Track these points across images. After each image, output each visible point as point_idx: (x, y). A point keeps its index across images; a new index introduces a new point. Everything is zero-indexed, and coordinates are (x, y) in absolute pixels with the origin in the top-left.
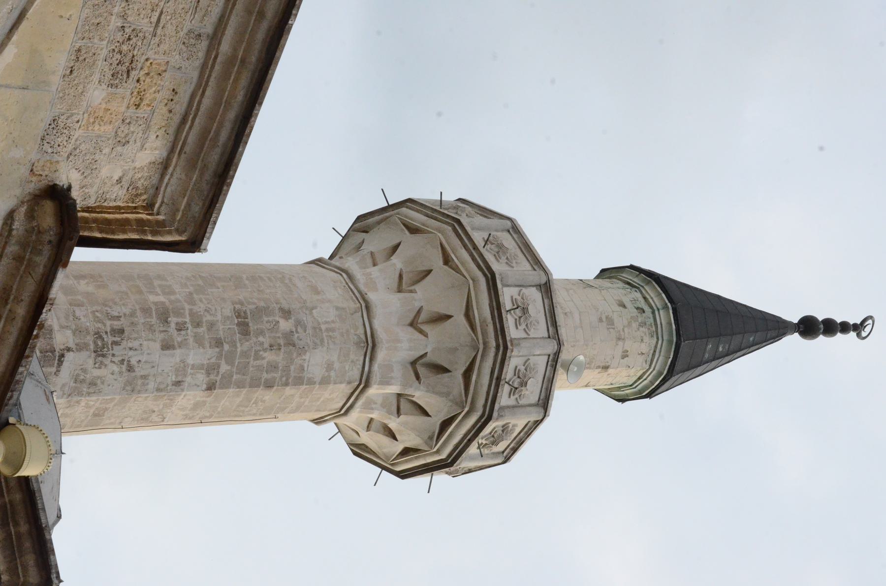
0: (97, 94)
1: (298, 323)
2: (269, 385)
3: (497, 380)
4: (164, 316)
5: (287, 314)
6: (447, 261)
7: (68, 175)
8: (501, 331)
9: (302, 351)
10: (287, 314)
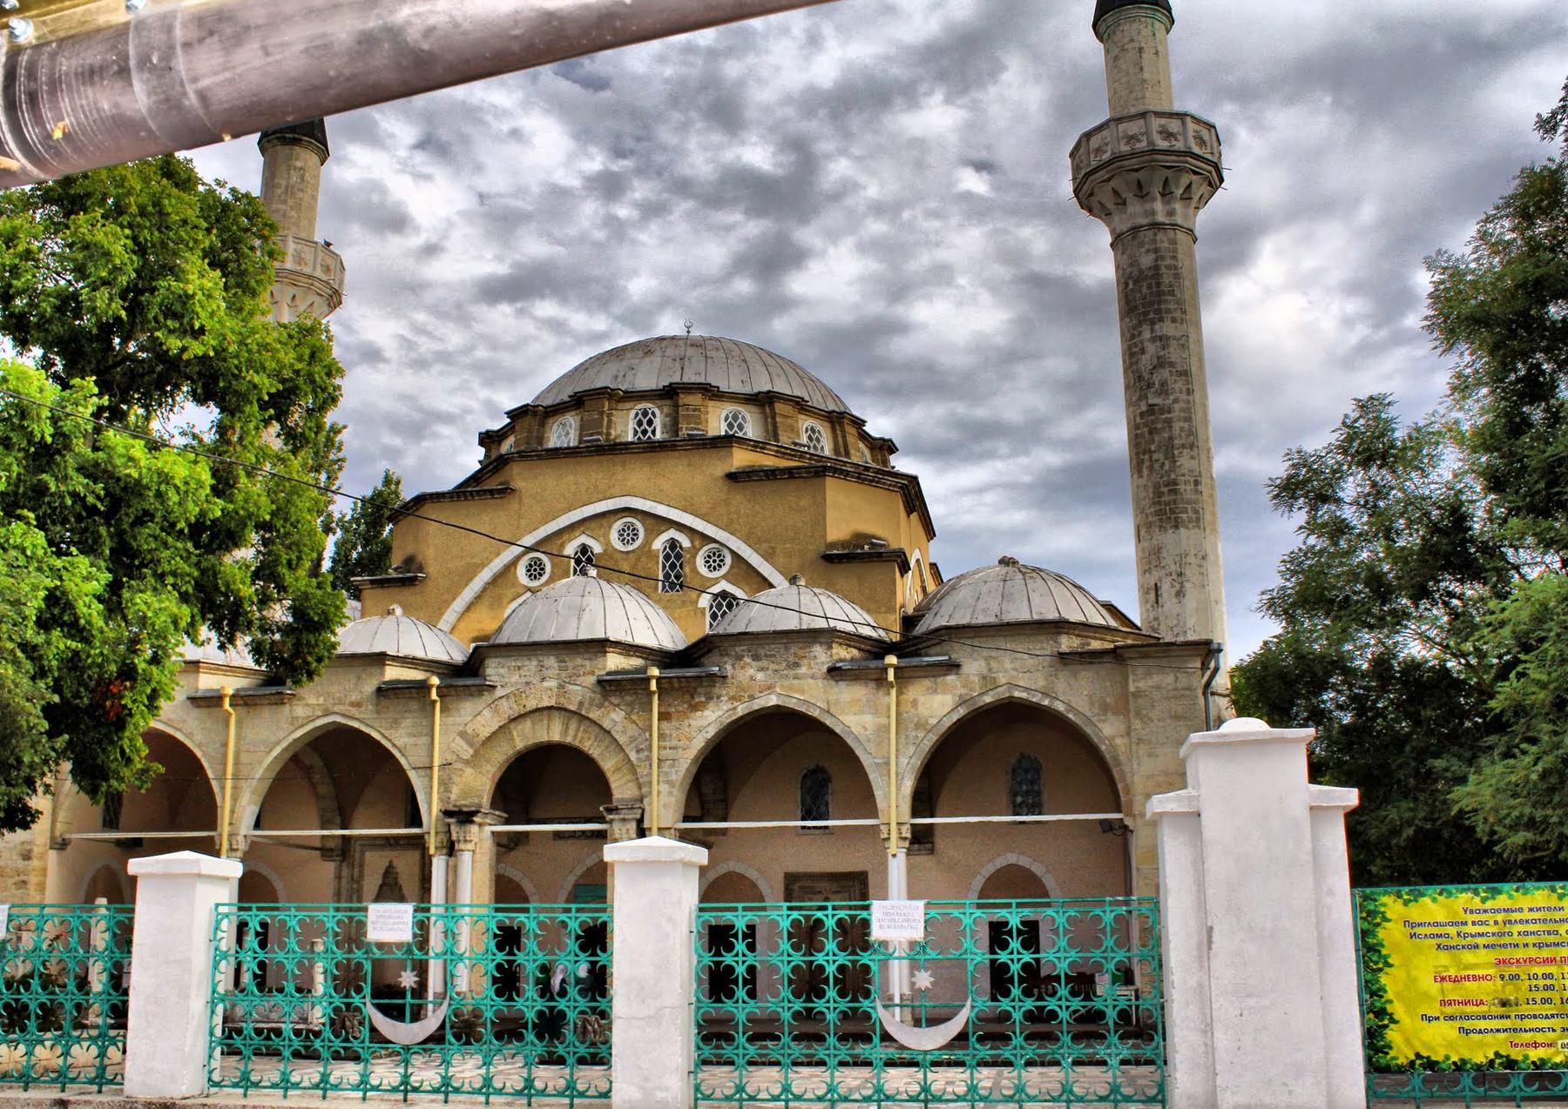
0: (803, 670)
1: (1130, 277)
2: (1158, 285)
3: (1133, 155)
4: (1132, 355)
5: (1127, 284)
6: (1091, 194)
7: (825, 668)
8: (1109, 163)
9: (1141, 272)
10: (1127, 284)
